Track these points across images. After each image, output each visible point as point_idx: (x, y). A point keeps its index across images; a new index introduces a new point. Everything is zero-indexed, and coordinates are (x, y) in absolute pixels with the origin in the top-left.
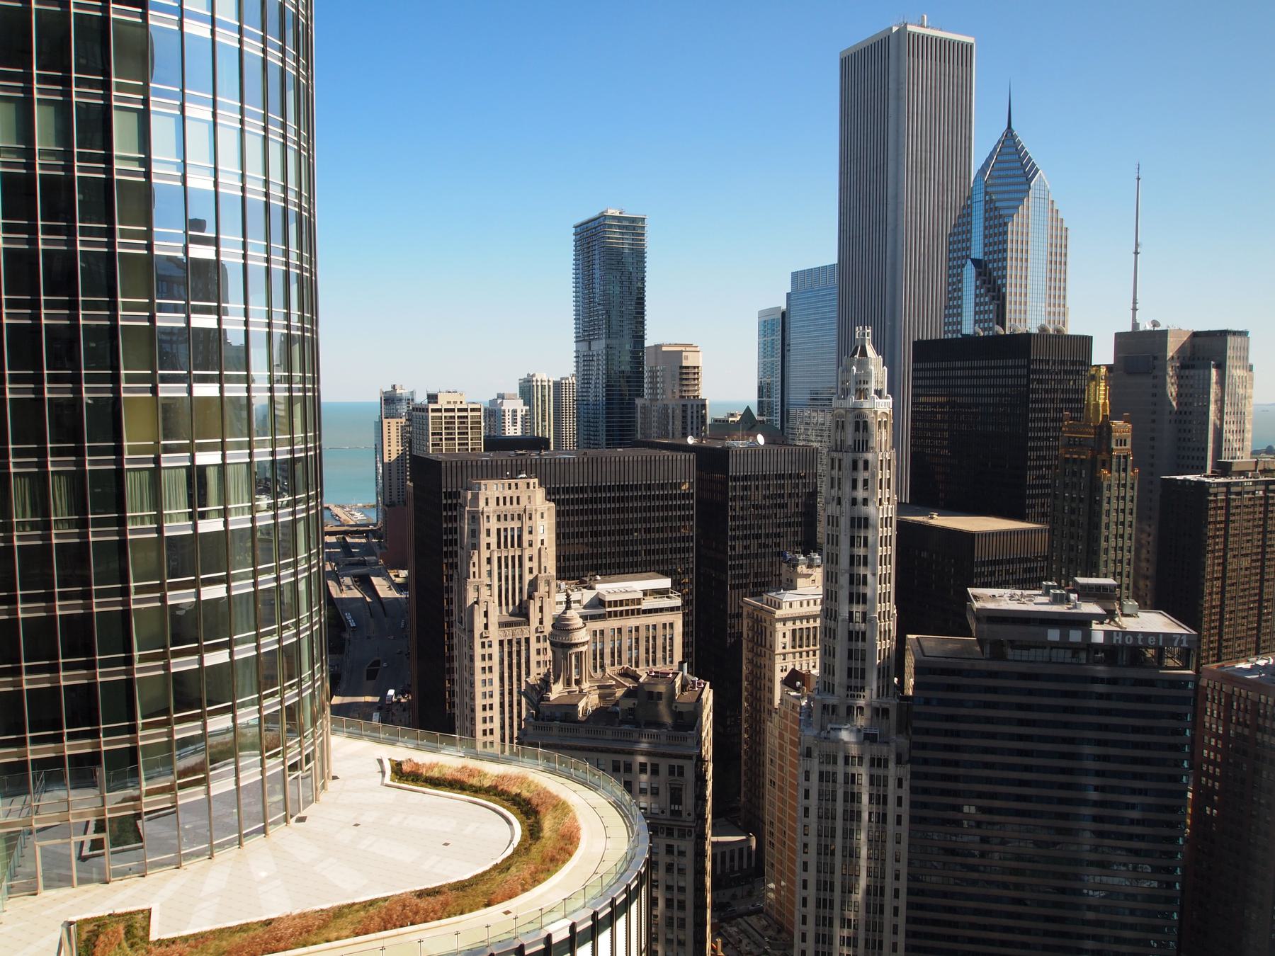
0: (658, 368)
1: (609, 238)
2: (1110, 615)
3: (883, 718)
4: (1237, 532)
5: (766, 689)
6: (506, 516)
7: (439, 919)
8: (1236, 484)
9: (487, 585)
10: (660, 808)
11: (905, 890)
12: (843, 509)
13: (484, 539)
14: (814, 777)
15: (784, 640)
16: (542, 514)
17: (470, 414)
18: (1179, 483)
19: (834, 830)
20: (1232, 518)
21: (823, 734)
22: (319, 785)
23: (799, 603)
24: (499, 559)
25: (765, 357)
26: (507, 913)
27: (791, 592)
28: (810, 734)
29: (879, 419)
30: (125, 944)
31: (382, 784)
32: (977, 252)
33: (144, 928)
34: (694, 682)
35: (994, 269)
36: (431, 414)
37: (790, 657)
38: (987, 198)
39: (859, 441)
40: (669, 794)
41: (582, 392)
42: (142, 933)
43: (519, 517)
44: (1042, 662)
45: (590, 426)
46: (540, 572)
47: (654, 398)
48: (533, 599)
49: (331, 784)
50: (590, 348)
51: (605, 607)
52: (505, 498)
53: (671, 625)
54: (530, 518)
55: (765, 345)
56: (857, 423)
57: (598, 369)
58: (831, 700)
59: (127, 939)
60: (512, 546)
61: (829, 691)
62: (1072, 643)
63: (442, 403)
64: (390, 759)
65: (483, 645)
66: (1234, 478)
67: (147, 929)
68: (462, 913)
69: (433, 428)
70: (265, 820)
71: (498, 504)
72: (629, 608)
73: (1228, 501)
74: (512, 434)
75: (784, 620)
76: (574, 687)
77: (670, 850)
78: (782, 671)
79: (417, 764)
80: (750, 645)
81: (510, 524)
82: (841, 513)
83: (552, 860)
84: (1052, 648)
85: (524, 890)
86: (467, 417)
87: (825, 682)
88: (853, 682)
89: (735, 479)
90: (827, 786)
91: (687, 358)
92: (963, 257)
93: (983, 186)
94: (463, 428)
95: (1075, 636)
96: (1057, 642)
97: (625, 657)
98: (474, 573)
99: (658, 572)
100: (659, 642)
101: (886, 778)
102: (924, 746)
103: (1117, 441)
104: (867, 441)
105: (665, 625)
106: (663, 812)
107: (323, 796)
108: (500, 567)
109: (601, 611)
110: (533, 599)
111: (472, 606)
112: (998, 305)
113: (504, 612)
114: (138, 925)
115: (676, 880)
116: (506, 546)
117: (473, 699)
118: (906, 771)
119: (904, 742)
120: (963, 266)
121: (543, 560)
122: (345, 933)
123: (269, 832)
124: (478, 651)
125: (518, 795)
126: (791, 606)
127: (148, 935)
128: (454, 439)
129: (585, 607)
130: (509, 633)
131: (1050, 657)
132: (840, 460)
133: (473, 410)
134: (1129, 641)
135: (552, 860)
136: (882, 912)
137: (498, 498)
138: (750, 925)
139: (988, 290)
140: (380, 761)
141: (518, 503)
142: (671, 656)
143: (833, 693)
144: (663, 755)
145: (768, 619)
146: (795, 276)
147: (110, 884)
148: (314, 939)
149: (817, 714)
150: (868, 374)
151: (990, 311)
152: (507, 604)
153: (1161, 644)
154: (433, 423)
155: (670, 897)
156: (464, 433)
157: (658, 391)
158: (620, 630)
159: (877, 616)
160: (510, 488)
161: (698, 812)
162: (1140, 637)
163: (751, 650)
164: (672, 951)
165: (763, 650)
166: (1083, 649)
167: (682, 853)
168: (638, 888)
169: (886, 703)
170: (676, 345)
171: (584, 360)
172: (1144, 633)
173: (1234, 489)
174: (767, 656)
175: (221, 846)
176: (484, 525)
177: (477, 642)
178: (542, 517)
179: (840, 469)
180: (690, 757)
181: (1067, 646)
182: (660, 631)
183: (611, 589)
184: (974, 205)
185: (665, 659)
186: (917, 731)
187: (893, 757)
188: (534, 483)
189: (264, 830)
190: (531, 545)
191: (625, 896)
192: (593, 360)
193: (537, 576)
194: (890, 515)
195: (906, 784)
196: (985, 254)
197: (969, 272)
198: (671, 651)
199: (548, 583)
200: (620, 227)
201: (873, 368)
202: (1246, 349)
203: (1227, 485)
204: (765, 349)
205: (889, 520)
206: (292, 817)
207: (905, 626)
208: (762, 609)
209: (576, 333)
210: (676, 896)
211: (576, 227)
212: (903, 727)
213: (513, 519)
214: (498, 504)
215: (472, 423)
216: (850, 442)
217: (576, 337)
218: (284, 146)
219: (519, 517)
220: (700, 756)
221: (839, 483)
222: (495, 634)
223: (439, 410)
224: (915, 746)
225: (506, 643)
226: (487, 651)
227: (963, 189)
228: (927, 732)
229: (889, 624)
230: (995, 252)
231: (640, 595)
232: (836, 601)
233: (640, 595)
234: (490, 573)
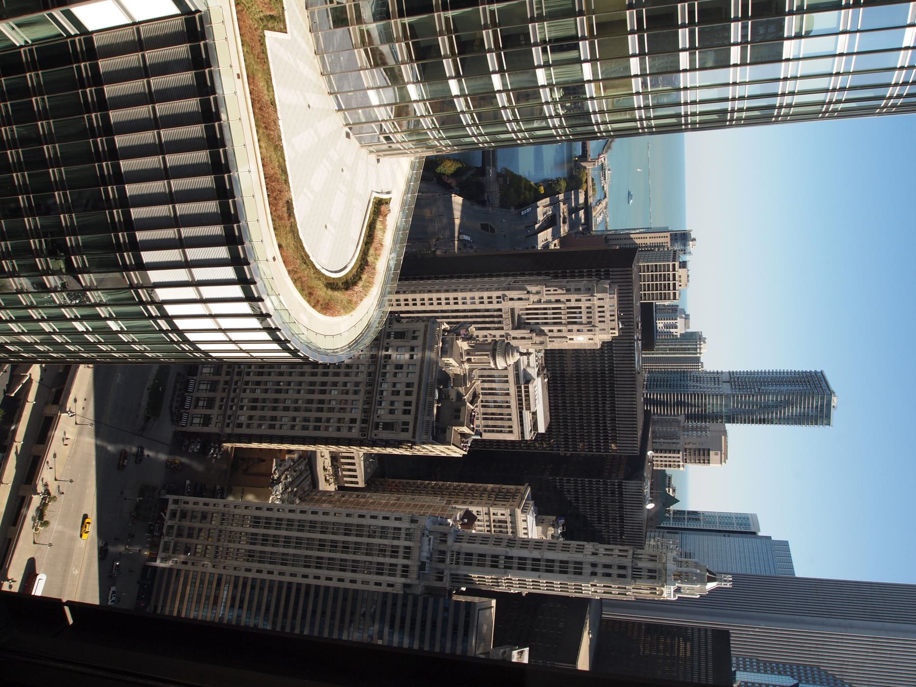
0: (708, 432)
1: (813, 397)
3: (436, 576)
5: (465, 500)
6: (591, 313)
7: (271, 213)
9: (540, 300)
10: (381, 415)
11: (319, 584)
12: (589, 557)
13: (573, 297)
14: (397, 524)
15: (499, 514)
16: (592, 339)
17: (671, 292)
19: (361, 536)
21: (427, 532)
22: (371, 149)
23: (526, 527)
24: (560, 308)
25: (719, 517)
26: (274, 259)
27: (534, 522)
28: (426, 522)
29: (657, 588)
30: (262, 15)
31: (372, 191)
33: (274, 28)
34: (467, 442)
36: (671, 264)
37: (486, 518)
39: (641, 572)
40: (390, 421)
41: (690, 376)
42: (270, 26)
43: (589, 323)
45: (664, 382)
46: (550, 337)
47: (686, 429)
48: (530, 332)
49: (373, 157)
50: (724, 382)
51: (525, 384)
52: (603, 312)
53: (511, 432)
54: (589, 330)
55: (729, 518)
56: (655, 571)
57: (708, 388)
58: (450, 540)
59: (265, 16)
60: (569, 318)
61: (457, 539)
63: (680, 272)
64: (391, 198)
65: (498, 297)
67: (273, 29)
68: (275, 229)
69: (660, 265)
70: (346, 110)
71: (599, 307)
72: (524, 401)
74: (659, 325)
75: (513, 515)
76: (465, 358)
77: (353, 421)
78: (478, 512)
79: (386, 215)
80: (497, 490)
81: (584, 316)
82: (586, 555)
83: (310, 294)
85: (289, 272)
86: (669, 290)
87: (463, 536)
88: (462, 556)
89: (620, 485)
90: (390, 533)
91: (716, 454)
94: (661, 287)
97: (489, 398)
98: (550, 291)
99: (551, 422)
100: (499, 423)
101: (394, 575)
102: (415, 605)
104: (641, 578)
105: (511, 427)
106: (378, 417)
107: (364, 151)
108: (554, 309)
109: (522, 381)
110: (530, 332)
111: (526, 289)
113: (521, 312)
114: (276, 24)
115: (333, 424)
116: (568, 313)
117: (461, 291)
118: (399, 590)
119: (419, 590)
120: (793, 677)
121: (559, 339)
122: (264, 150)
123: (339, 113)
124: (495, 294)
125: (360, 278)
126: (524, 521)
127: (268, 29)
128: (652, 281)
129: (524, 369)
130: (506, 316)
132: (626, 556)
133: (675, 294)
135: (310, 294)
136: (305, 566)
137: (603, 307)
138: (306, 478)
140: (388, 193)
141: (600, 322)
142: (489, 431)
143: (455, 542)
144: (416, 418)
145: (515, 503)
146: (785, 544)
147: (306, 11)
148: (261, 131)
149: (442, 529)
152: (527, 314)
154: (664, 265)
155: (323, 420)
156: (657, 288)
157: (690, 432)
158: (508, 394)
159: (509, 577)
160: (611, 315)
161: (377, 441)
163: (493, 490)
164: (289, 421)
165: (493, 499)
167: (350, 429)
168: (287, 350)
169: (446, 579)
170: (726, 447)
171: (716, 377)
174: (489, 502)
175: (329, 81)
176: (583, 297)
177: (500, 293)
178: (589, 339)
179: (619, 556)
180: (414, 437)
182: (507, 423)
183: (538, 389)
185: (487, 426)
186: (426, 601)
187: (408, 581)
188: (615, 333)
189: (340, 109)
190: (569, 331)
191: (293, 349)
192: (715, 384)
193: (547, 335)
194: (584, 592)
195: (389, 590)
198: (493, 431)
199: (542, 343)
200: (822, 405)
201: (698, 586)
204: (726, 517)
205: (580, 591)
206: (350, 129)
207: (502, 597)
208: (522, 500)
209: (736, 372)
210: (323, 425)
211: (822, 372)
212: (430, 591)
213: (588, 318)
214: (599, 307)
215: (665, 293)
216: (640, 564)
217: (733, 372)
218: (826, 91)
219: (589, 323)
220: (414, 444)
221: (608, 555)
222: (506, 305)
223: (674, 270)
224: (416, 597)
225: (499, 313)
226: (494, 300)
228: (425, 607)
229: (503, 586)
231: (533, 410)
232: (521, 547)
233: (533, 410)
234: (549, 302)
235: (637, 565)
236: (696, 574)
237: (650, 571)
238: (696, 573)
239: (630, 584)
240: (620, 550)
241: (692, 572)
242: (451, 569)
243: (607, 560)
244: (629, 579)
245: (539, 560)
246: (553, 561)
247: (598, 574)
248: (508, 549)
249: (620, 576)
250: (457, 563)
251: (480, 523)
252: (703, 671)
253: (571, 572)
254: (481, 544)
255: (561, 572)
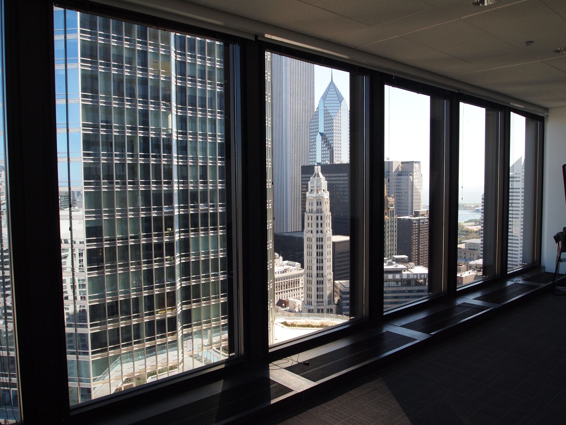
2: (407, 269)
4: (423, 237)
8: (422, 219)
12: (314, 235)
18: (402, 219)
20: (421, 232)
29: (325, 201)
32: (321, 130)
35: (329, 137)
38: (325, 109)
39: (318, 209)
44: (387, 287)
56: (318, 202)
58: (311, 307)
61: (309, 304)
62: (397, 279)
66: (421, 217)
73: (419, 226)
84: (389, 282)
88: (319, 300)
92: (316, 132)
93: (323, 104)
95: (398, 276)
96: (391, 279)
103: (390, 205)
104: (321, 209)
112: (331, 151)
120: (316, 135)
131: (389, 285)
132: (311, 216)
134: (415, 277)
139: (327, 145)
143: (311, 305)
150: (321, 184)
151: (328, 154)
153: (426, 277)
162: (419, 275)
166: (400, 281)
169: (331, 307)
172: (420, 274)
173: (421, 221)
179: (312, 220)
181: (395, 280)
184: (319, 111)
196: (325, 131)
197: (319, 138)
202: (420, 168)
203: (419, 220)
216: (315, 209)
221: (311, 225)
227: (311, 104)
230: (329, 130)
235: (315, 211)
236: (317, 182)
237: (318, 205)
238: (317, 183)
239: (325, 214)
240: (308, 219)
241: (316, 185)
242: (326, 305)
243: (314, 226)
244: (323, 215)
245: (317, 260)
246: (317, 253)
247: (322, 229)
248: (313, 276)
249: (321, 219)
250: (322, 302)
251: (283, 297)
252: (338, 178)
253: (322, 243)
254: (311, 291)
255: (322, 248)
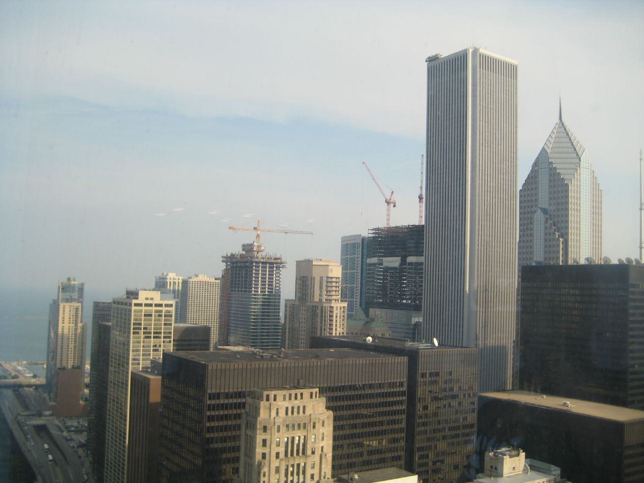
16: (323, 422)
52: (293, 408)
54: (314, 427)
91: (332, 271)
137: (287, 408)
141: (304, 412)
184: (540, 171)
190: (313, 453)
223: (140, 305)
